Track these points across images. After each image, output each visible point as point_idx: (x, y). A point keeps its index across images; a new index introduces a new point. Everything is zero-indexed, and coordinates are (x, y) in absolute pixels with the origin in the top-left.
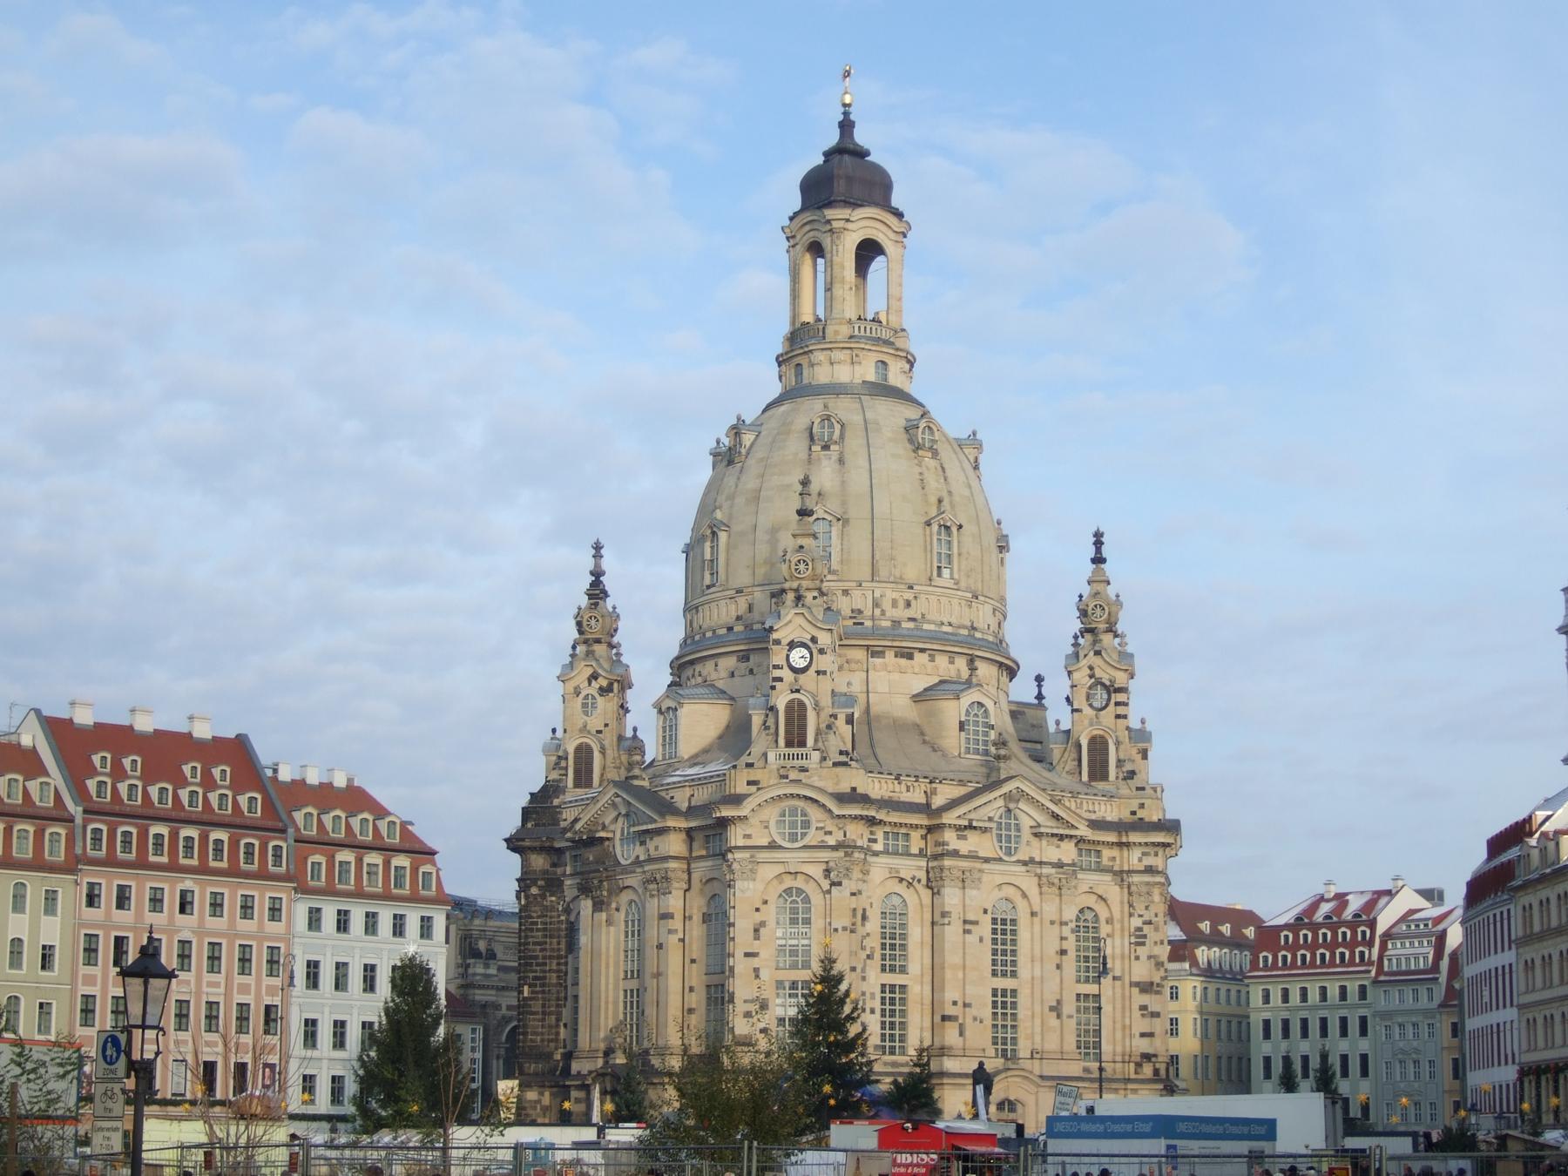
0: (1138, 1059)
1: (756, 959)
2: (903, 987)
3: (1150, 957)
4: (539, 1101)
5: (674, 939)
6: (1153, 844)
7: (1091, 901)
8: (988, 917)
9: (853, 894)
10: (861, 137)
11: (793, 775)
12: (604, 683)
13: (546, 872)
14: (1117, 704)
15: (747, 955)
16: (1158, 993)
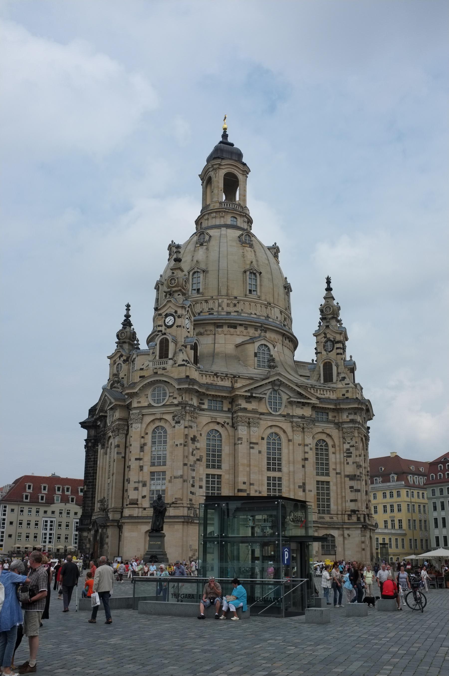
0: (349, 513)
1: (141, 462)
2: (219, 476)
3: (353, 463)
4: (87, 537)
5: (120, 456)
6: (352, 408)
7: (324, 437)
8: (265, 441)
9: (186, 427)
10: (230, 140)
11: (160, 372)
12: (125, 358)
13: (96, 436)
14: (337, 348)
15: (136, 459)
16: (358, 480)
